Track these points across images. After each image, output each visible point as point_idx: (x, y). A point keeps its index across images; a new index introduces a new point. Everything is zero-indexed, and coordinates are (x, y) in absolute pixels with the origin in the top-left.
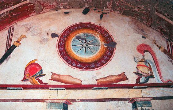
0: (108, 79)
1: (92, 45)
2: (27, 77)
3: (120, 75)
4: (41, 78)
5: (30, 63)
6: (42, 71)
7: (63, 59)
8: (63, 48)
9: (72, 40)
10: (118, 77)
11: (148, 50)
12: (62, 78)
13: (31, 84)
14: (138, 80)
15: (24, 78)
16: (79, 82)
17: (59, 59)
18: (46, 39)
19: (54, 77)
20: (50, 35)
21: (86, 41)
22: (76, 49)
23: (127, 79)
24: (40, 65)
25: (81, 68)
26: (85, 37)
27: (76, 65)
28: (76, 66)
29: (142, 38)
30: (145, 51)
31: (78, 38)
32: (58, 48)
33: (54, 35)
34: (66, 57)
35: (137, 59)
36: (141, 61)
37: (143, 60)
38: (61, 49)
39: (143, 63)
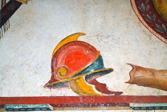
2: (62, 77)
4: (101, 80)
5: (66, 42)
6: (100, 60)
7: (155, 31)
8: (148, 7)
13: (75, 95)
15: (53, 79)
17: (144, 31)
19: (139, 74)
24: (92, 47)
32: (134, 5)
34: (161, 26)
38: (144, 8)
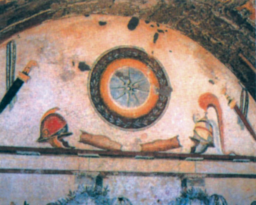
0: (156, 145)
1: (138, 88)
3: (171, 140)
4: (66, 139)
5: (48, 114)
6: (66, 127)
9: (111, 77)
10: (168, 143)
11: (214, 104)
12: (93, 140)
14: (193, 149)
15: (41, 137)
16: (118, 148)
18: (71, 72)
19: (85, 137)
20: (77, 65)
21: (130, 82)
22: (117, 94)
23: (179, 146)
25: (121, 126)
26: (129, 74)
27: (115, 120)
28: (115, 123)
29: (208, 83)
30: (210, 105)
31: (119, 74)
33: (83, 67)
35: (196, 117)
36: (201, 121)
37: (204, 120)
39: (203, 124)
